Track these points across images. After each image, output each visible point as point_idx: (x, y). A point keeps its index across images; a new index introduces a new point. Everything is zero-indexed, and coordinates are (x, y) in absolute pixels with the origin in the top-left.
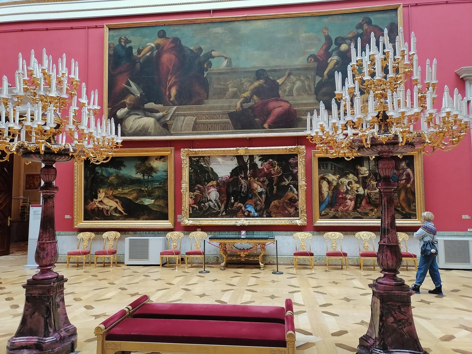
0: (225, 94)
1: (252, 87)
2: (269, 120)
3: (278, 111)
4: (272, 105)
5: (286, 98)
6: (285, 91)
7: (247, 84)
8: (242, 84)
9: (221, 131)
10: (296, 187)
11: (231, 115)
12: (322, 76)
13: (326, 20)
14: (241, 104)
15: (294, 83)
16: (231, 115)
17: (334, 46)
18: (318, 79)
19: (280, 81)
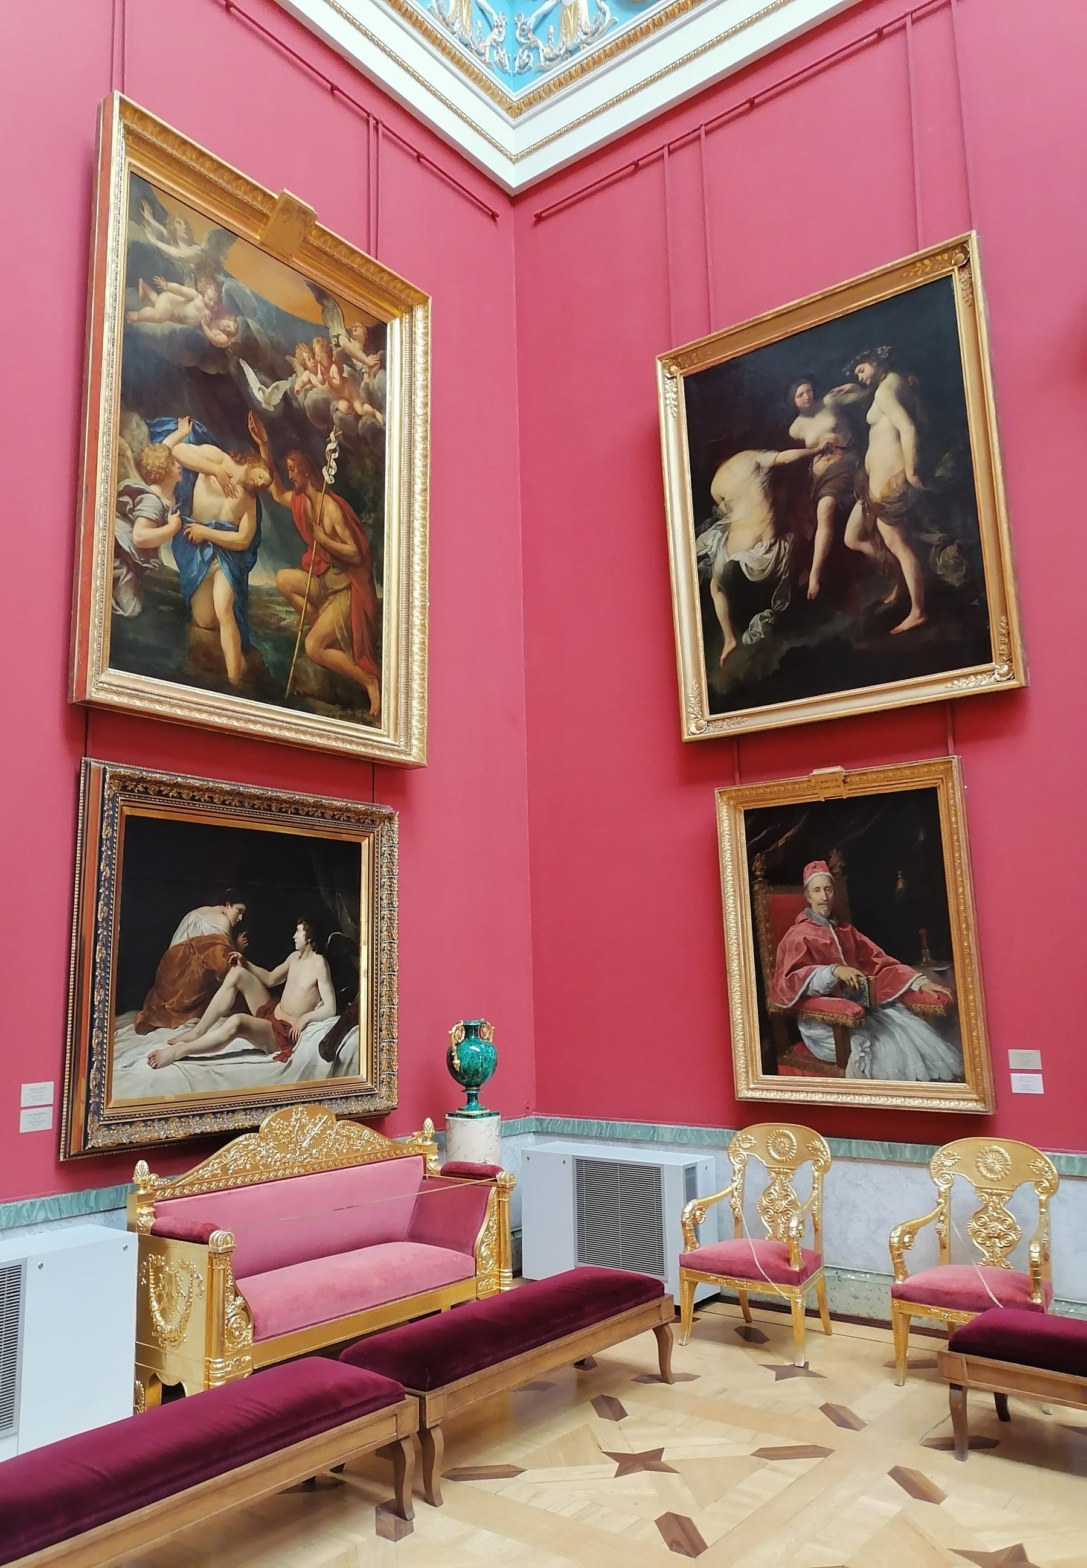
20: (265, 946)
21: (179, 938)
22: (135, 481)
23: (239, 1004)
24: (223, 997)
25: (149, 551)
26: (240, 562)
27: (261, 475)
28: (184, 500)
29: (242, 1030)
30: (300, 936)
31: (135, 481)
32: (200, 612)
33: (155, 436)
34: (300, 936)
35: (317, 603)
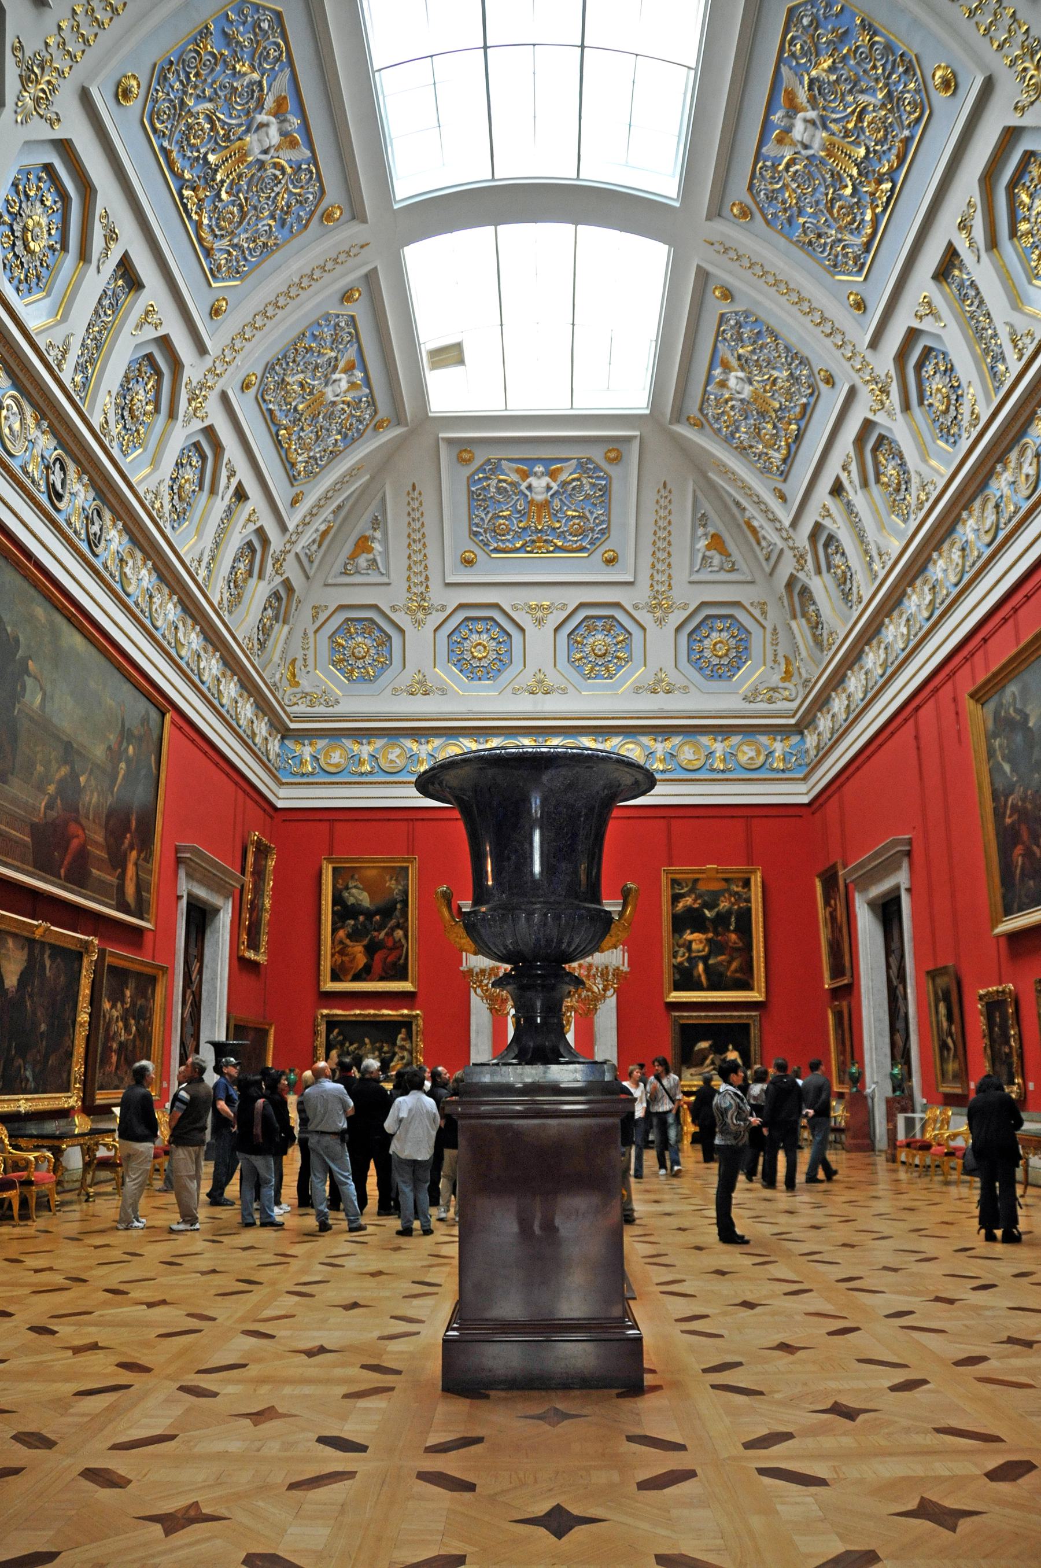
0: (32, 774)
1: (57, 777)
2: (66, 862)
3: (75, 843)
4: (73, 828)
5: (84, 821)
6: (84, 806)
7: (54, 766)
8: (50, 761)
9: (18, 864)
10: (74, 1021)
11: (35, 830)
12: (112, 793)
13: (127, 687)
14: (47, 807)
15: (92, 793)
16: (35, 830)
17: (125, 744)
18: (110, 799)
19: (82, 779)
20: (719, 1049)
21: (696, 1048)
22: (677, 949)
23: (713, 1063)
24: (708, 1061)
25: (681, 963)
26: (705, 959)
27: (710, 935)
28: (689, 949)
29: (714, 1069)
30: (731, 1047)
31: (677, 949)
32: (695, 974)
33: (681, 937)
34: (731, 1047)
35: (730, 963)
